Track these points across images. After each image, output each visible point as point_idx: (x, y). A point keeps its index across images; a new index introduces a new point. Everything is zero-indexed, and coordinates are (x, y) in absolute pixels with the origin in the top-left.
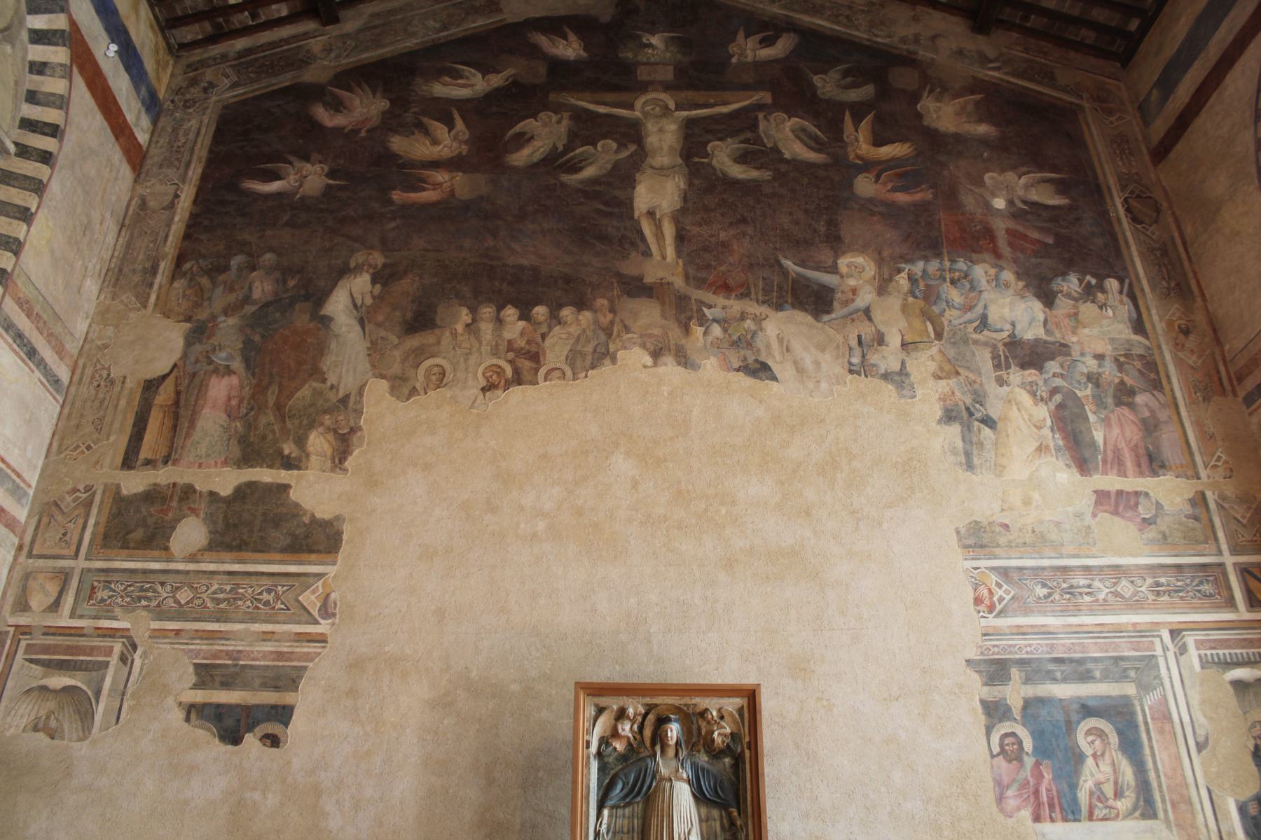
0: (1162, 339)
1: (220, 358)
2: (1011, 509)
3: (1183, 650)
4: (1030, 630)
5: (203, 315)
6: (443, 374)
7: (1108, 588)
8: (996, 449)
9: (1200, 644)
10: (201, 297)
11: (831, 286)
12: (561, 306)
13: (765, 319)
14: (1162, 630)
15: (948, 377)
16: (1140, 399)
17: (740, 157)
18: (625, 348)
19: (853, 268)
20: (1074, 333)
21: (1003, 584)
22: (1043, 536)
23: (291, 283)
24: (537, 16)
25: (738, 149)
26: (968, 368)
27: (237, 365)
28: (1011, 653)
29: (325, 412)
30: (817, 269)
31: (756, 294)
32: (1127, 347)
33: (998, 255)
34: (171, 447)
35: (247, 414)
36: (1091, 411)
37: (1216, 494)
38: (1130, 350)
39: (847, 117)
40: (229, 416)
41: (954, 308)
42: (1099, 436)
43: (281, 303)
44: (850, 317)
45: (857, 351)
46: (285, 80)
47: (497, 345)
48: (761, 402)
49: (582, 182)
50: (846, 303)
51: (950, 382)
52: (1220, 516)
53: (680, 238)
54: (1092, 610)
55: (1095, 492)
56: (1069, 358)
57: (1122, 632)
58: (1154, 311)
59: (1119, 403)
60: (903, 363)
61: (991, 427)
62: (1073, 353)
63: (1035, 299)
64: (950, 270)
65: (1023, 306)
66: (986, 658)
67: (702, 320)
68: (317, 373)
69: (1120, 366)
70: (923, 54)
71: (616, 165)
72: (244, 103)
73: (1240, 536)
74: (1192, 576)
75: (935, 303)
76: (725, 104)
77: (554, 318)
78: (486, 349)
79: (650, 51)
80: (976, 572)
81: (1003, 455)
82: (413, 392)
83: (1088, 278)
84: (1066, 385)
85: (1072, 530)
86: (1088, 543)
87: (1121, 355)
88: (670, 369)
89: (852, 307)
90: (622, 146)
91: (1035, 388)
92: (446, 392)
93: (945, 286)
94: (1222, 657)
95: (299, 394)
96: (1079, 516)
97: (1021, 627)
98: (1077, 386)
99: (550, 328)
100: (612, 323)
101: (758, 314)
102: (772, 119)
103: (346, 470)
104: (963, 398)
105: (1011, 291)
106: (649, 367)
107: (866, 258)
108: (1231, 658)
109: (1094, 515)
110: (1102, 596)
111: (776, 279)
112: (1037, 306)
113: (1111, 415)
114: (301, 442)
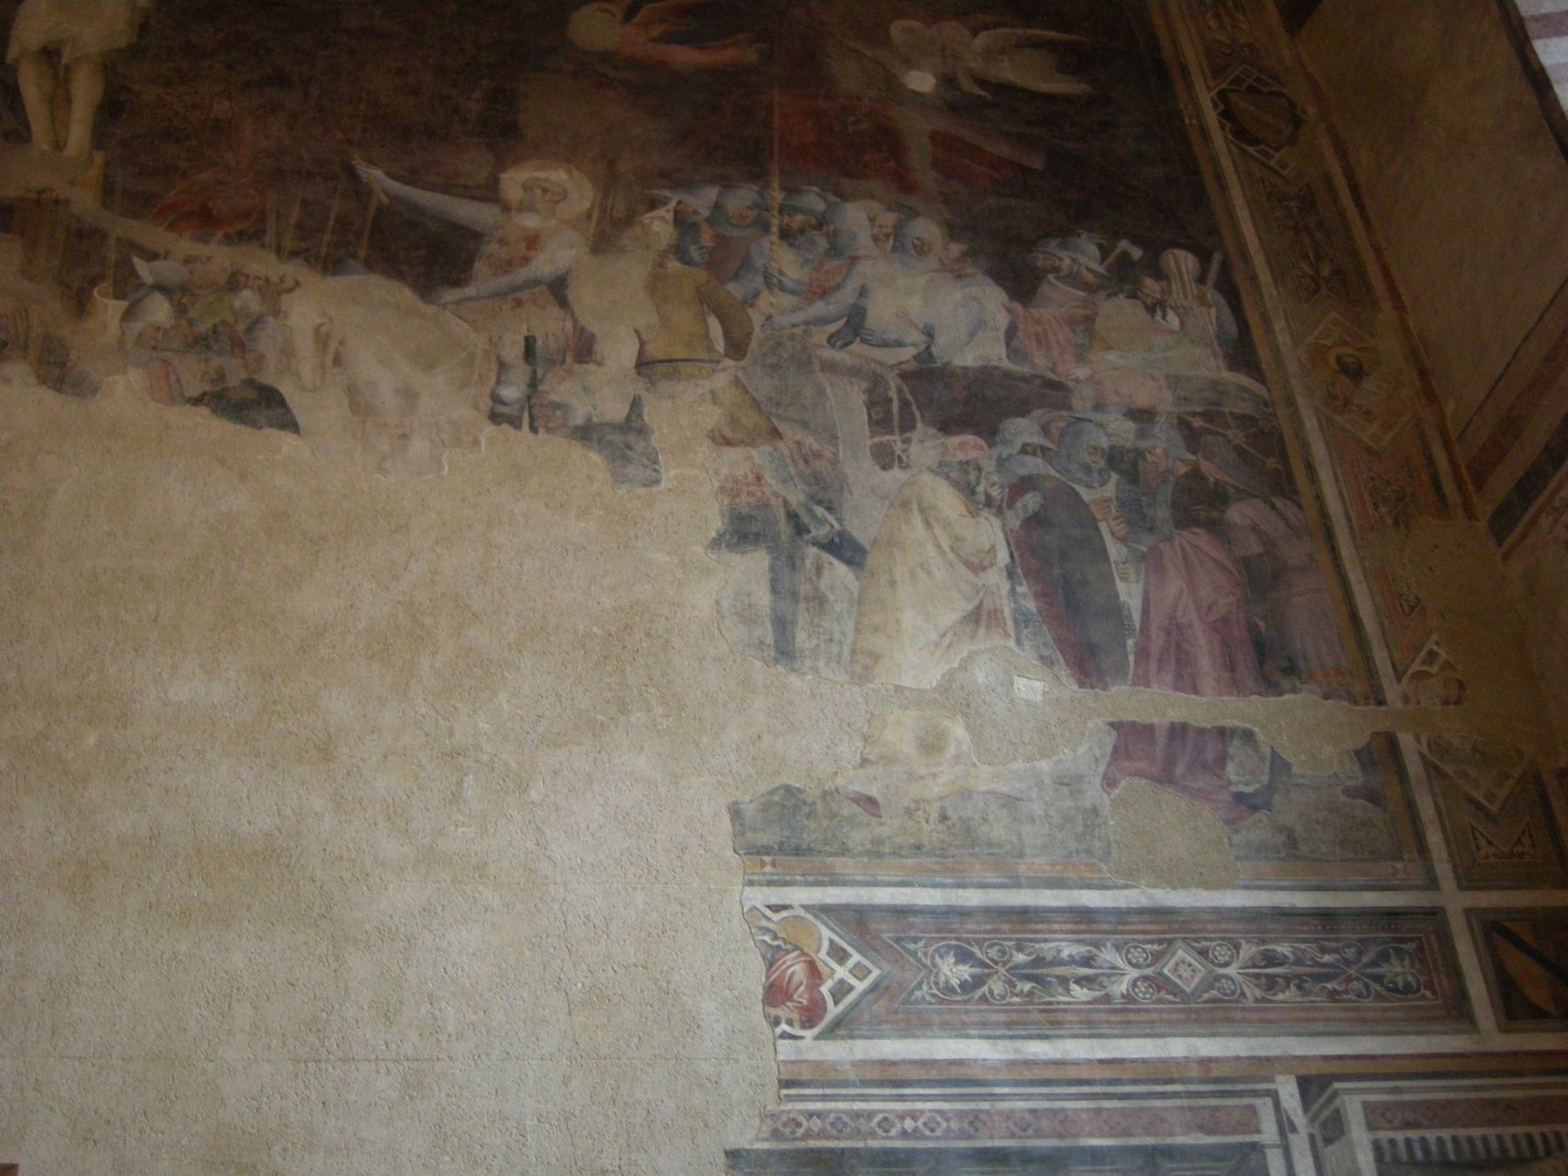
2: (888, 760)
3: (1332, 1129)
8: (861, 614)
9: (1376, 1116)
11: (475, 228)
13: (291, 290)
14: (1279, 1078)
15: (750, 441)
16: (1237, 514)
19: (538, 191)
20: (1081, 358)
21: (850, 949)
22: (969, 831)
26: (805, 425)
28: (858, 1134)
30: (447, 189)
33: (904, 183)
36: (1113, 534)
37: (1424, 740)
38: (1214, 404)
41: (783, 289)
42: (1130, 593)
44: (515, 297)
45: (520, 374)
48: (243, 477)
50: (508, 265)
51: (754, 453)
52: (1433, 794)
53: (111, 108)
54: (1090, 1023)
56: (1065, 414)
58: (1279, 325)
59: (1185, 519)
60: (636, 404)
61: (849, 562)
62: (1076, 403)
63: (989, 280)
64: (783, 210)
65: (958, 295)
66: (785, 1146)
67: (127, 286)
69: (1192, 438)
73: (1483, 842)
74: (1360, 941)
75: (736, 277)
80: (776, 917)
81: (876, 629)
83: (1124, 244)
84: (1052, 472)
85: (1047, 816)
86: (1089, 852)
87: (1194, 414)
89: (521, 274)
91: (972, 476)
93: (765, 242)
94: (1434, 1148)
96: (1069, 783)
97: (893, 1063)
98: (1079, 475)
101: (275, 279)
104: (783, 492)
107: (576, 173)
108: (1458, 1151)
109: (1109, 782)
110: (1120, 987)
112: (993, 300)
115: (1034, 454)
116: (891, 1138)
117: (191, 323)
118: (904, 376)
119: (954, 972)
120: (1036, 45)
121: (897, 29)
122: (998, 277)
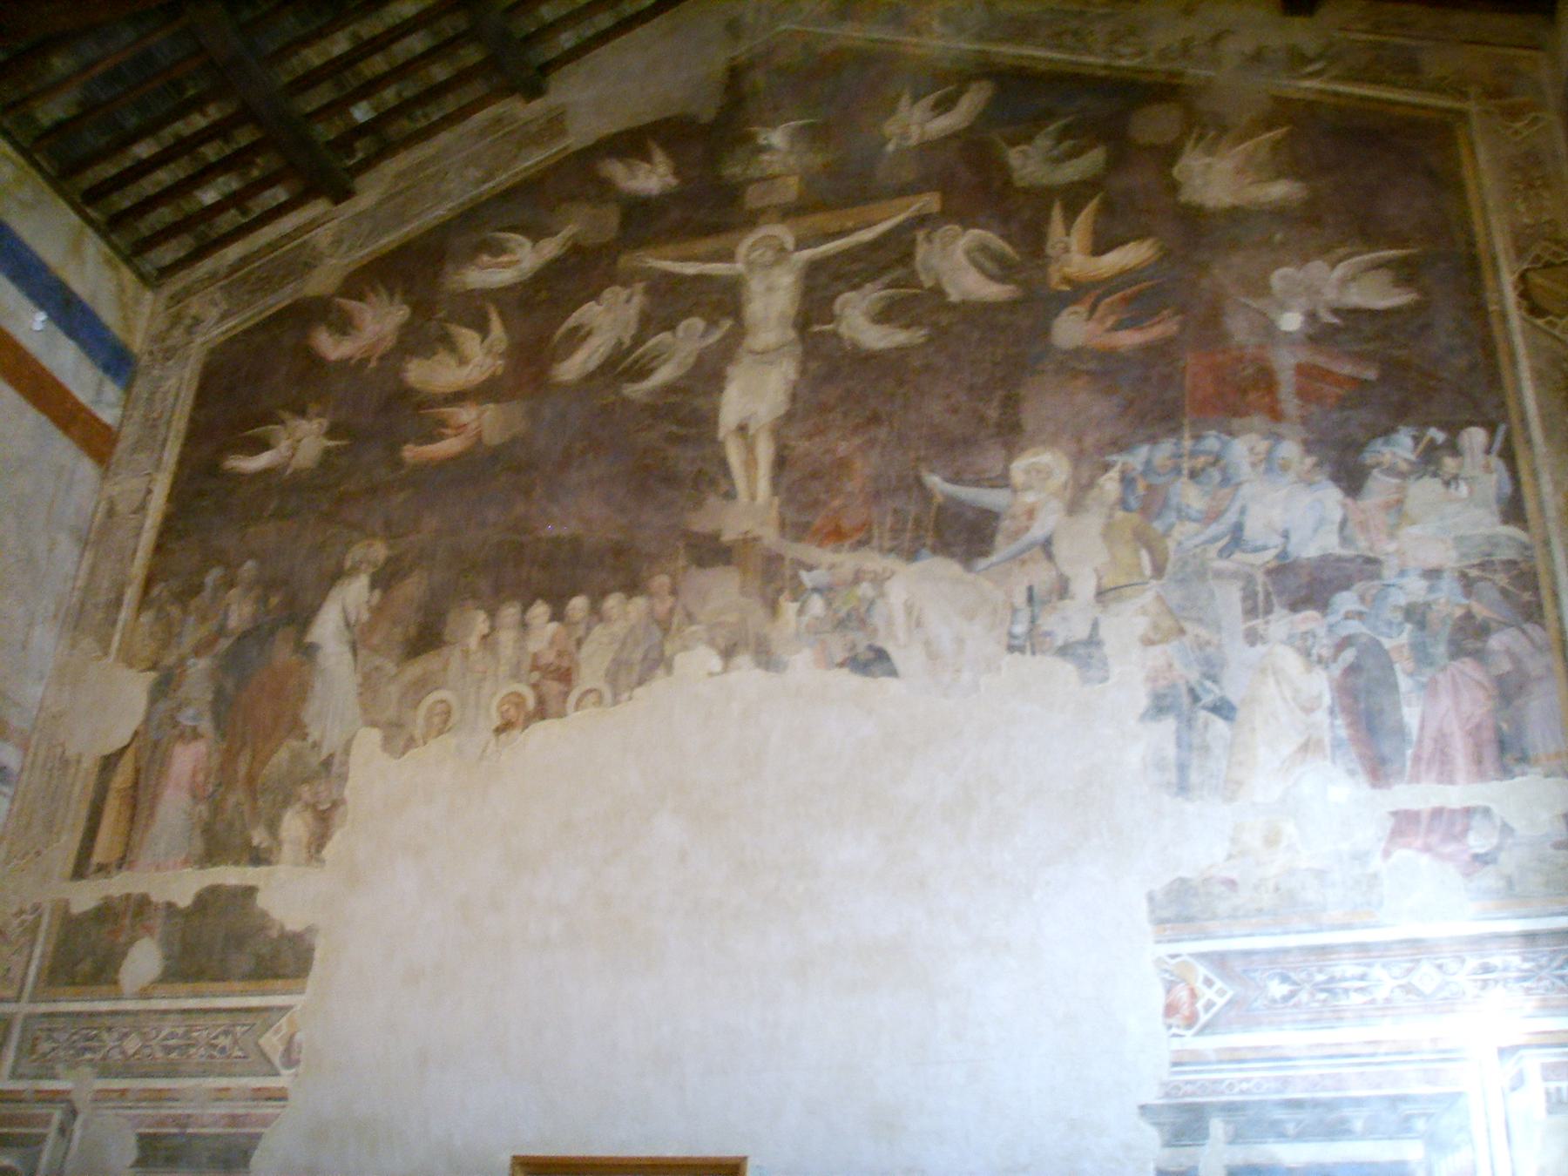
0: (1553, 527)
1: (186, 718)
4: (1251, 1055)
5: (170, 659)
6: (448, 713)
7: (1395, 978)
10: (168, 635)
12: (604, 594)
13: (889, 578)
15: (1165, 640)
16: (1496, 642)
17: (881, 313)
18: (685, 648)
20: (1392, 536)
23: (275, 601)
24: (614, 130)
25: (881, 298)
26: (1200, 621)
27: (206, 725)
28: (1214, 1092)
29: (306, 781)
30: (977, 483)
31: (881, 537)
32: (1486, 548)
33: (1276, 414)
34: (127, 844)
35: (214, 791)
36: (1404, 671)
38: (1489, 555)
39: (1057, 214)
40: (194, 797)
41: (1189, 519)
42: (1411, 715)
43: (258, 635)
44: (1019, 558)
45: (1024, 615)
46: (283, 298)
47: (519, 663)
49: (651, 393)
50: (1015, 535)
53: (781, 462)
55: (1395, 814)
56: (1376, 582)
57: (1410, 1053)
59: (1457, 651)
67: (799, 592)
68: (297, 728)
69: (1467, 583)
70: (1195, 73)
71: (700, 360)
72: (232, 341)
75: (1159, 515)
76: (869, 225)
77: (596, 612)
78: (504, 669)
79: (766, 157)
82: (410, 743)
84: (1364, 629)
87: (1473, 566)
88: (746, 672)
90: (712, 323)
91: (1309, 643)
92: (449, 740)
93: (1178, 485)
95: (275, 760)
96: (1360, 857)
98: (1385, 629)
99: (589, 629)
100: (671, 611)
102: (937, 236)
103: (322, 861)
105: (1291, 476)
106: (718, 674)
111: (913, 510)
112: (1331, 496)
113: (1440, 677)
114: (273, 826)
115: (1353, 618)
116: (1233, 1094)
117: (836, 611)
118: (1269, 572)
119: (1278, 989)
120: (1378, 266)
121: (1278, 278)
122: (1336, 479)
